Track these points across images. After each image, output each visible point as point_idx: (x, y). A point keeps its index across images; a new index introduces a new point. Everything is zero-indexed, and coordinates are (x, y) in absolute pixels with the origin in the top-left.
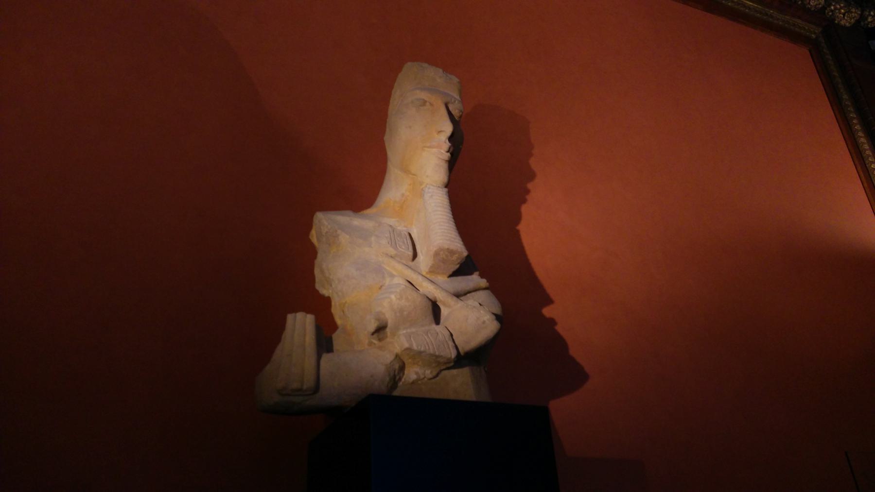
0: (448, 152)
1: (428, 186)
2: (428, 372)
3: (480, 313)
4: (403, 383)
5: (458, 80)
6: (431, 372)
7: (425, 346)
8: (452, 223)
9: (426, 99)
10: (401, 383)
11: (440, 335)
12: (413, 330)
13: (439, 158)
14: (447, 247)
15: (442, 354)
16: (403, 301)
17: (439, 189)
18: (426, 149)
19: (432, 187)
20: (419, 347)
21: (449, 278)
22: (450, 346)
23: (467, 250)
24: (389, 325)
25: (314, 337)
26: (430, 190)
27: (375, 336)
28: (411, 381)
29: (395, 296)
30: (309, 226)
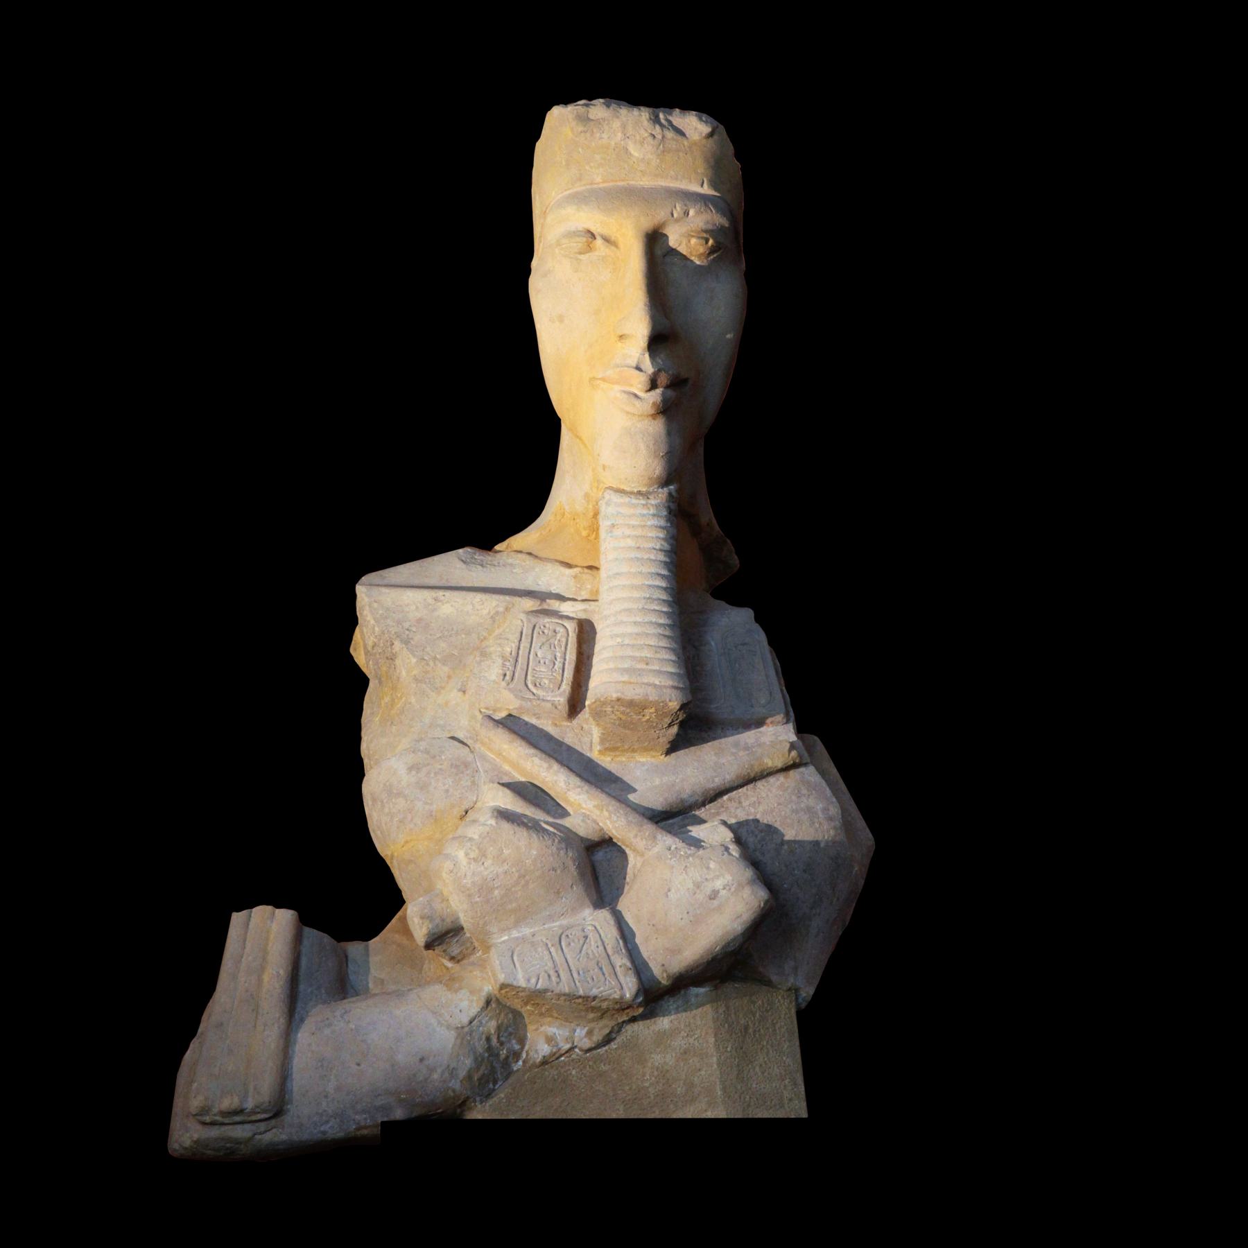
2: (580, 1032)
3: (708, 868)
4: (524, 1062)
6: (590, 1033)
7: (549, 976)
10: (520, 1063)
11: (593, 937)
12: (526, 931)
14: (615, 696)
15: (595, 992)
16: (488, 863)
19: (616, 498)
20: (533, 981)
21: (682, 755)
22: (618, 969)
24: (465, 920)
25: (282, 972)
27: (438, 950)
28: (538, 1058)
29: (467, 854)
30: (350, 621)
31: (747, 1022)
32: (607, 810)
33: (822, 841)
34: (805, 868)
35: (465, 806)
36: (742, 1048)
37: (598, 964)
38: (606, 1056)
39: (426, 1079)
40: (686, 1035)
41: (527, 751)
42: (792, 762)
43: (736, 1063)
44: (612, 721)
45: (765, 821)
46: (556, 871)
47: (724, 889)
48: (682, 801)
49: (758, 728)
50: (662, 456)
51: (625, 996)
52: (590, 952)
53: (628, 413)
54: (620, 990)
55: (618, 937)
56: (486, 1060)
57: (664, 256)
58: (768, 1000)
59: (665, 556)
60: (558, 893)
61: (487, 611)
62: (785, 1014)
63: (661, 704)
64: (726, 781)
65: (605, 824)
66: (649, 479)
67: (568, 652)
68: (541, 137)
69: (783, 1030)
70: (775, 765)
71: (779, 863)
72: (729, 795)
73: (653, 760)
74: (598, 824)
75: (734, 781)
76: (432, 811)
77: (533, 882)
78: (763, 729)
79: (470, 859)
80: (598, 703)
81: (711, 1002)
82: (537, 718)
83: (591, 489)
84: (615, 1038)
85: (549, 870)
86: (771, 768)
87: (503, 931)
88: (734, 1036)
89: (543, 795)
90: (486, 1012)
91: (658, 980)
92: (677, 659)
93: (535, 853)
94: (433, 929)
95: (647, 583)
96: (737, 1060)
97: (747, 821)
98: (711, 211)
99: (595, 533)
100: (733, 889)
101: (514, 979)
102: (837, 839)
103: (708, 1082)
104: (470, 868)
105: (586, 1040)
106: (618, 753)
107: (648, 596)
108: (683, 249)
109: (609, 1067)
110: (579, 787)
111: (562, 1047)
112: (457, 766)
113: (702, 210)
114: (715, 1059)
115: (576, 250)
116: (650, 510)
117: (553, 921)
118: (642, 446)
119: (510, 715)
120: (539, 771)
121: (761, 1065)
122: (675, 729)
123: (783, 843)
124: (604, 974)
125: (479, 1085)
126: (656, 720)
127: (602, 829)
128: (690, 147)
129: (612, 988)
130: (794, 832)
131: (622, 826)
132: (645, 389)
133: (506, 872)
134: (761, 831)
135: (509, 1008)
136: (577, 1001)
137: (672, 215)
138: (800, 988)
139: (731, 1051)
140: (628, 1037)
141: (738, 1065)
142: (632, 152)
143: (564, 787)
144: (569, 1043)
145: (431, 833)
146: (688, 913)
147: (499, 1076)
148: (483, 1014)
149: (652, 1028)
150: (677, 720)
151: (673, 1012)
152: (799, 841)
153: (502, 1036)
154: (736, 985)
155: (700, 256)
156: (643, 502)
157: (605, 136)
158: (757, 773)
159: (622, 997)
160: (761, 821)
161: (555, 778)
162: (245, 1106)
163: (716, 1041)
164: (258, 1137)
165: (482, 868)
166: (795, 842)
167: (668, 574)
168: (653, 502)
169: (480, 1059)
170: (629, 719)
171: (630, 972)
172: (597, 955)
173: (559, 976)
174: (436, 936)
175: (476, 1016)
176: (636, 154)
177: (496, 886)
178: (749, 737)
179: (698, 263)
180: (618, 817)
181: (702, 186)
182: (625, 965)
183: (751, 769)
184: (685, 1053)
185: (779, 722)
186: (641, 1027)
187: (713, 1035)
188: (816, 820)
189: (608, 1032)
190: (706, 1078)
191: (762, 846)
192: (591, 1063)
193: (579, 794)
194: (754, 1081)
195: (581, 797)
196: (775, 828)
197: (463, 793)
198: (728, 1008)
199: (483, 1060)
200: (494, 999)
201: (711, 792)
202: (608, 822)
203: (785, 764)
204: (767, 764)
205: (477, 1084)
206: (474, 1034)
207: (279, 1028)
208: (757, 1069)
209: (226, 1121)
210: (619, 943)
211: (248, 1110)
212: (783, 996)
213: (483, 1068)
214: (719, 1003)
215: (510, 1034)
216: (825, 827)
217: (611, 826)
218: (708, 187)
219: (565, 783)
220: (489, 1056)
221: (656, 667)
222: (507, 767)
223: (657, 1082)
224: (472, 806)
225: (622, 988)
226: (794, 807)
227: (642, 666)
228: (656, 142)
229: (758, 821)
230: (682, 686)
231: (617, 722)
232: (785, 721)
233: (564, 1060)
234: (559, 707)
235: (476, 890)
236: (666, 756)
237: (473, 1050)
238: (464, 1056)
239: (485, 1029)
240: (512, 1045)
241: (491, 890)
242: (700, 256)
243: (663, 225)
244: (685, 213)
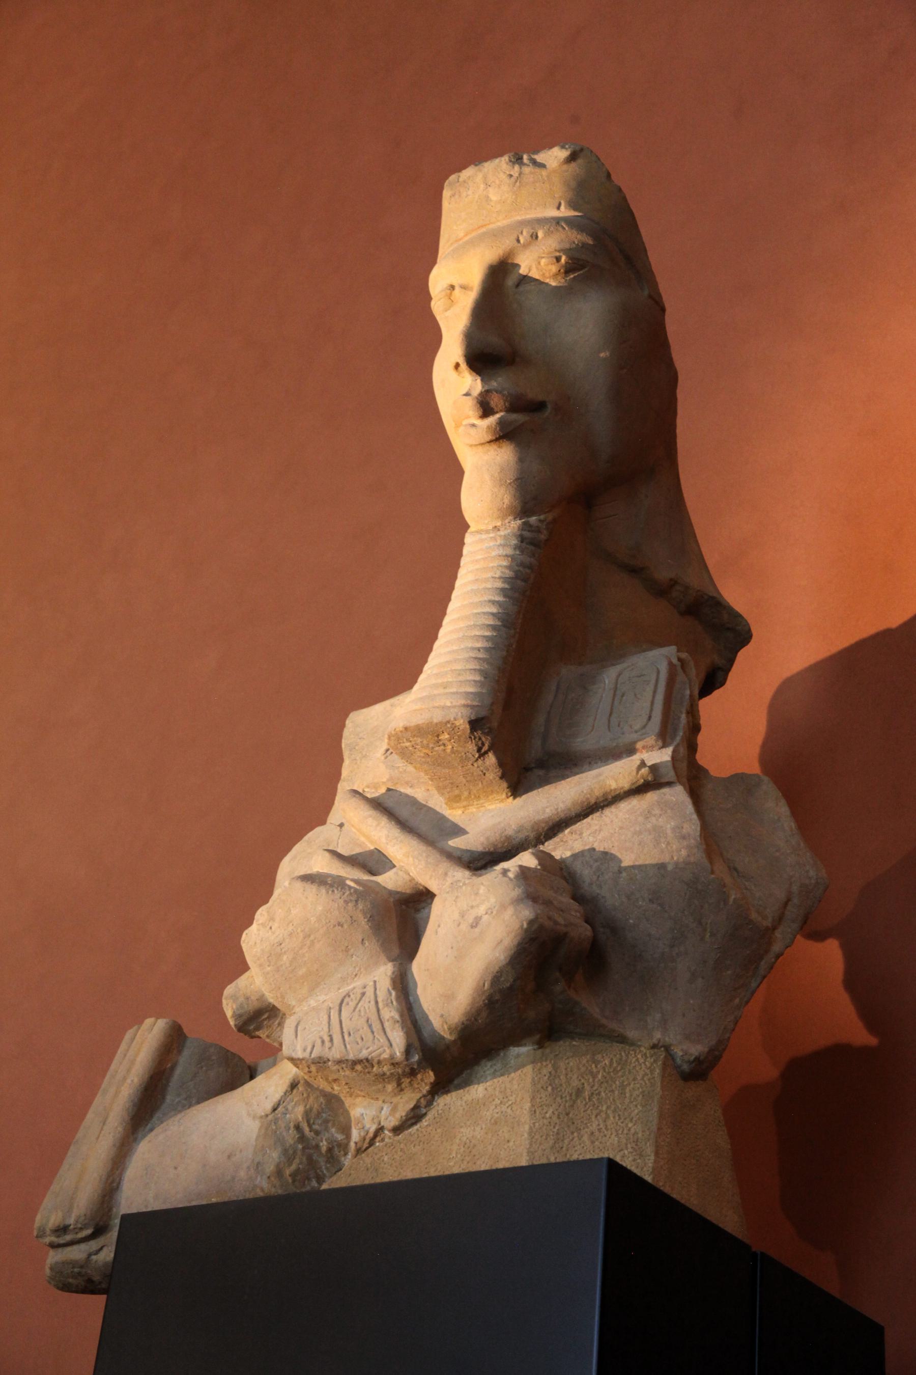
6: (394, 1109)
13: (471, 446)
31: (583, 1084)
33: (669, 863)
34: (650, 897)
36: (567, 1114)
37: (368, 1021)
38: (416, 1136)
39: (233, 1178)
40: (499, 1101)
42: (642, 781)
43: (555, 1130)
45: (602, 849)
46: (342, 926)
47: (486, 913)
48: (508, 838)
49: (629, 756)
50: (510, 484)
51: (396, 1054)
52: (362, 1009)
53: (471, 446)
54: (388, 1048)
55: (390, 988)
56: (299, 1153)
57: (518, 286)
58: (621, 1059)
59: (503, 582)
60: (347, 950)
62: (646, 1074)
63: (449, 725)
64: (559, 810)
66: (499, 510)
69: (637, 1092)
70: (621, 785)
71: (619, 895)
72: (571, 828)
73: (502, 805)
74: (409, 874)
75: (569, 809)
77: (319, 941)
81: (533, 1062)
82: (411, 787)
84: (425, 1114)
85: (335, 926)
86: (615, 790)
87: (300, 1001)
88: (558, 1099)
89: (385, 859)
90: (290, 1096)
91: (439, 1033)
92: (483, 679)
93: (320, 909)
94: (238, 1009)
95: (475, 611)
96: (557, 1128)
97: (582, 853)
98: (564, 228)
100: (495, 912)
101: (293, 1051)
102: (692, 859)
103: (515, 1154)
104: (259, 934)
105: (390, 1118)
107: (472, 623)
108: (535, 274)
109: (418, 1147)
110: (396, 838)
111: (370, 1128)
113: (552, 229)
114: (527, 1127)
116: (497, 541)
117: (347, 984)
118: (487, 477)
119: (389, 790)
121: (592, 1133)
122: (491, 759)
123: (620, 870)
124: (373, 1032)
125: (294, 1181)
126: (460, 749)
127: (412, 879)
128: (548, 176)
129: (382, 1047)
130: (633, 857)
133: (291, 934)
134: (596, 861)
135: (317, 1089)
136: (621, 1130)
137: (518, 241)
138: (671, 1045)
139: (551, 1118)
140: (440, 1112)
141: (558, 1134)
144: (374, 1123)
146: (452, 948)
147: (325, 1172)
148: (288, 1099)
149: (465, 1098)
151: (489, 1078)
152: (640, 866)
153: (314, 1123)
154: (574, 1043)
155: (555, 276)
157: (470, 192)
158: (597, 798)
159: (392, 1057)
160: (597, 850)
162: (67, 1223)
163: (533, 1106)
164: (94, 1257)
165: (270, 933)
166: (633, 867)
167: (504, 600)
168: (502, 533)
169: (291, 1152)
171: (397, 1025)
172: (368, 1011)
173: (331, 1040)
174: (245, 1018)
175: (280, 1101)
177: (283, 951)
179: (554, 284)
181: (559, 208)
182: (392, 1017)
183: (590, 794)
184: (496, 1123)
185: (652, 747)
186: (454, 1099)
187: (529, 1100)
188: (663, 840)
189: (412, 1106)
190: (513, 1150)
191: (599, 877)
192: (402, 1146)
194: (576, 1151)
196: (612, 854)
198: (556, 1068)
199: (295, 1152)
200: (302, 1082)
203: (633, 784)
205: (290, 1181)
206: (280, 1122)
207: (113, 1137)
208: (585, 1138)
209: (61, 1241)
210: (390, 994)
211: (72, 1227)
212: (645, 1054)
213: (297, 1161)
214: (544, 1064)
215: (326, 1121)
216: (674, 846)
218: (566, 208)
220: (304, 1148)
221: (454, 690)
222: (362, 839)
223: (463, 1160)
225: (391, 1045)
226: (638, 829)
227: (441, 691)
228: (513, 179)
229: (594, 849)
230: (477, 704)
232: (660, 743)
233: (378, 1146)
235: (266, 958)
237: (280, 1141)
238: (270, 1149)
239: (292, 1115)
240: (333, 1136)
241: (279, 956)
243: (510, 254)
244: (532, 236)
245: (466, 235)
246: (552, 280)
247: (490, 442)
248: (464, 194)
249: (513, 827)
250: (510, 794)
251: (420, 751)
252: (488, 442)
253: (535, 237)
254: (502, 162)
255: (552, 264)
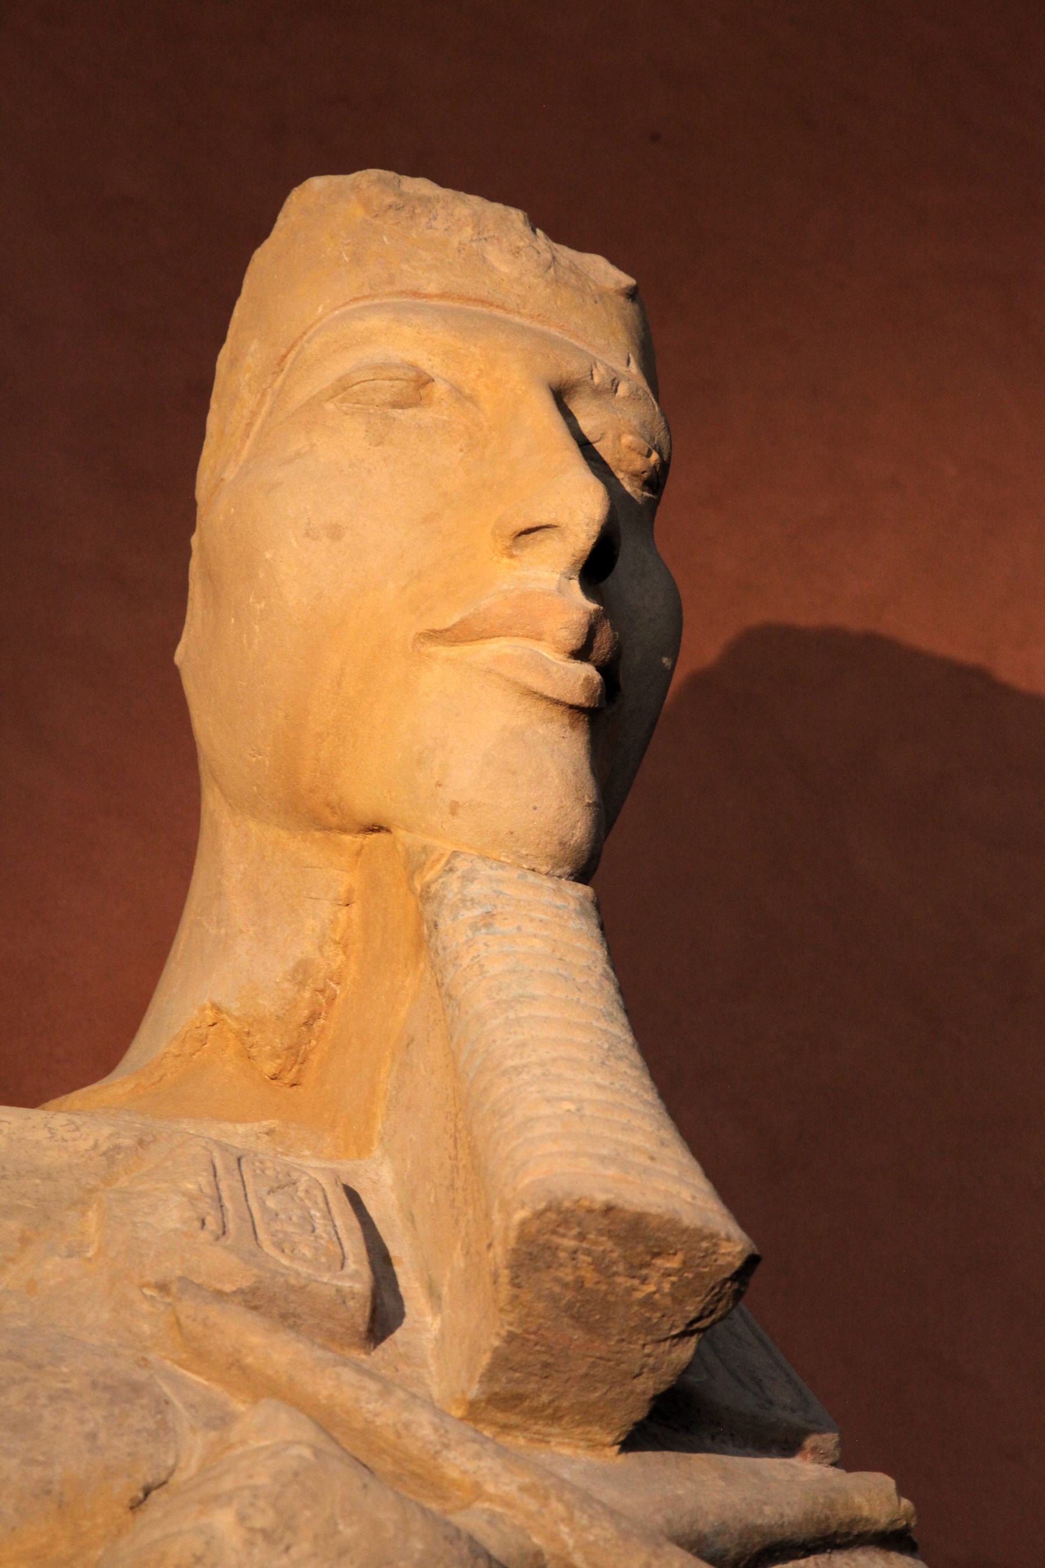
0: (581, 654)
1: (462, 865)
5: (627, 281)
8: (623, 1067)
9: (429, 363)
14: (601, 1198)
17: (531, 878)
18: (443, 651)
23: (744, 1225)
26: (474, 889)
29: (242, 1519)
32: (560, 1499)
35: (145, 1475)
41: (319, 1353)
44: (557, 1289)
50: (589, 805)
61: (91, 1142)
63: (704, 1244)
65: (554, 1537)
67: (335, 1211)
68: (274, 233)
70: (876, 1515)
76: (50, 1482)
78: (796, 1461)
79: (252, 1530)
80: (552, 1216)
83: (320, 949)
99: (296, 1067)
104: (250, 1554)
106: (514, 1419)
112: (106, 1388)
115: (388, 397)
120: (357, 1400)
126: (668, 1301)
131: (606, 1540)
132: (570, 648)
142: (497, 264)
143: (433, 1437)
145: (44, 1540)
150: (712, 1312)
155: (634, 475)
156: (554, 886)
161: (405, 1416)
170: (603, 1287)
176: (504, 269)
178: (771, 1466)
180: (591, 1517)
193: (478, 1456)
195: (482, 1464)
197: (136, 1444)
201: (757, 1539)
202: (564, 1529)
204: (860, 1508)
217: (571, 1542)
219: (436, 1430)
224: (163, 1477)
227: (648, 1162)
231: (569, 1295)
234: (351, 1303)
236: (621, 1451)
242: (634, 475)
245: (442, 296)
246: (627, 480)
247: (575, 709)
248: (424, 221)
249: (711, 1518)
250: (622, 1439)
251: (576, 1268)
252: (571, 707)
253: (615, 384)
254: (516, 216)
255: (639, 453)
